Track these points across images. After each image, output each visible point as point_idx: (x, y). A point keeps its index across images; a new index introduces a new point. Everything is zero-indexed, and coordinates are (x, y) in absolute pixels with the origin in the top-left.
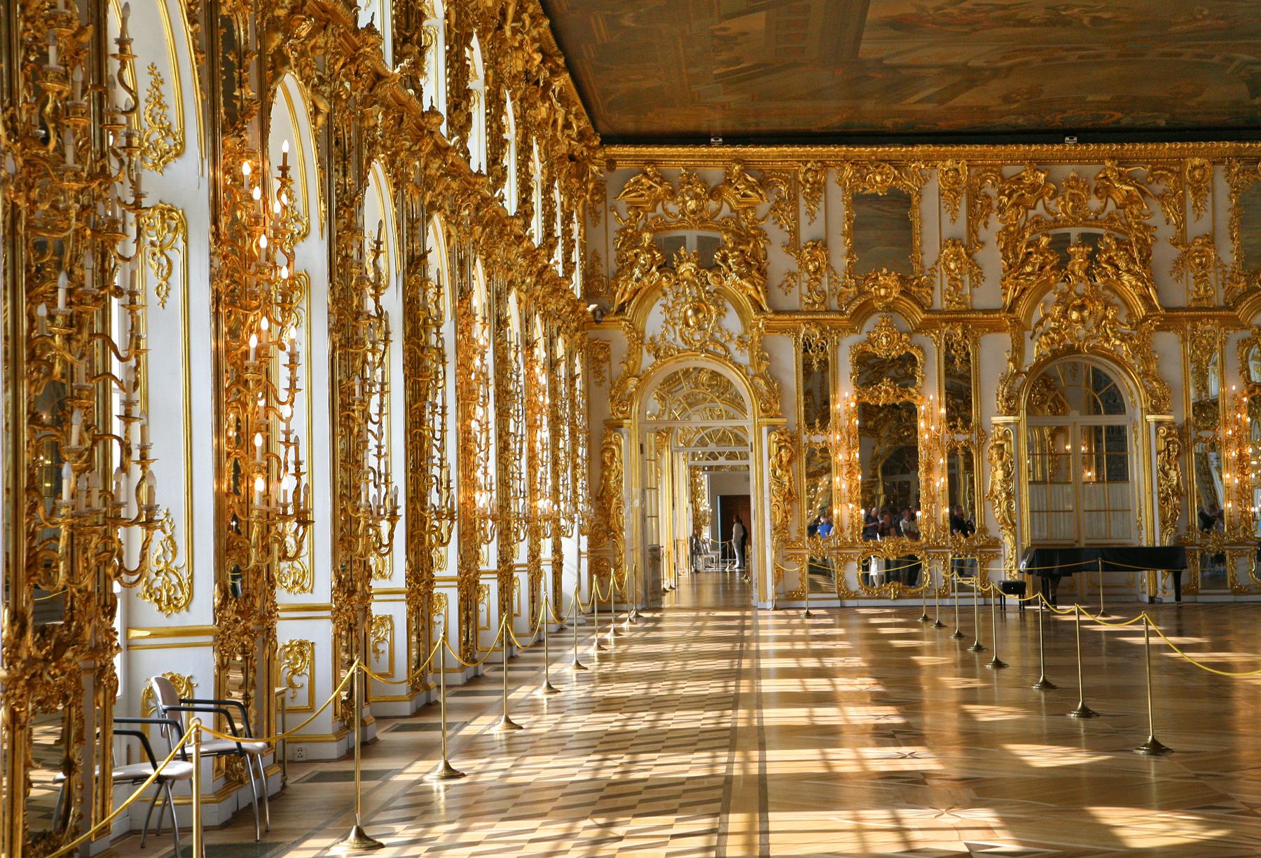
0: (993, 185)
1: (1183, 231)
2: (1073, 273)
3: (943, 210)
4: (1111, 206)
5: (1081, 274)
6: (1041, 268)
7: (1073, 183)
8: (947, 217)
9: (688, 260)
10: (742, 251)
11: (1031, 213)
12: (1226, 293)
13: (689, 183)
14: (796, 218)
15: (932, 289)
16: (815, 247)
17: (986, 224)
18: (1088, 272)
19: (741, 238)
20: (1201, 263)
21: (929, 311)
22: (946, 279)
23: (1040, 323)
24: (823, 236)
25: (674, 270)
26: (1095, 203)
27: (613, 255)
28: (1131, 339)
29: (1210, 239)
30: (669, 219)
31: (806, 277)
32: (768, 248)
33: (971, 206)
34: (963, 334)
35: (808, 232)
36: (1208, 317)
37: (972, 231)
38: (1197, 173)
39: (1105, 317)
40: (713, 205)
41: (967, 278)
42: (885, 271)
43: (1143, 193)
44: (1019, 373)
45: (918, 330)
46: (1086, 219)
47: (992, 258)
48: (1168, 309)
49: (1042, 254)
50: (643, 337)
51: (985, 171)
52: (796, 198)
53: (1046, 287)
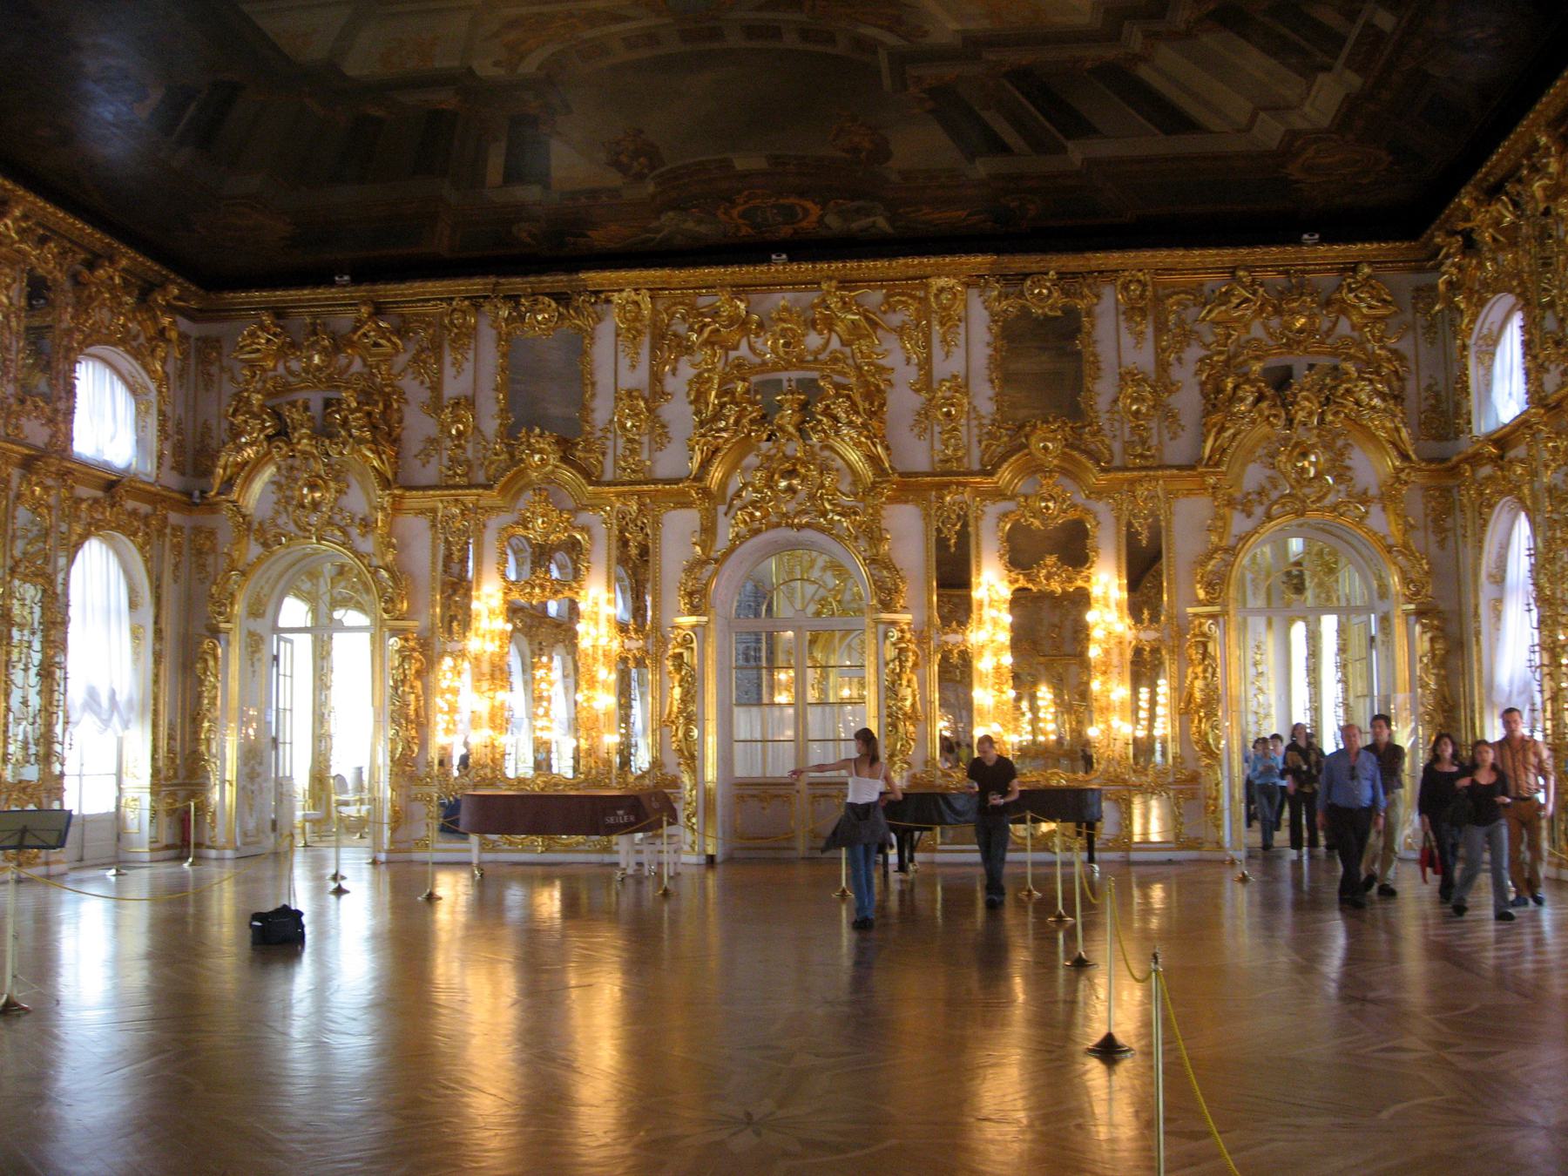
0: (684, 318)
1: (929, 374)
2: (781, 428)
3: (621, 355)
4: (835, 343)
5: (791, 429)
6: (737, 423)
7: (785, 315)
8: (624, 363)
9: (302, 426)
10: (369, 414)
11: (733, 354)
12: (983, 453)
13: (316, 334)
14: (441, 370)
15: (604, 454)
16: (458, 403)
17: (674, 371)
18: (800, 430)
19: (366, 397)
20: (948, 414)
21: (598, 483)
22: (621, 442)
23: (738, 495)
24: (470, 393)
25: (289, 443)
26: (813, 340)
27: (225, 425)
28: (856, 513)
29: (962, 385)
30: (291, 379)
31: (449, 443)
32: (406, 409)
33: (654, 348)
34: (640, 510)
35: (454, 386)
36: (959, 484)
37: (656, 377)
38: (943, 296)
39: (822, 486)
40: (342, 360)
41: (645, 439)
42: (537, 431)
43: (874, 325)
44: (706, 562)
45: (584, 508)
46: (801, 360)
47: (678, 412)
48: (901, 475)
49: (737, 404)
50: (250, 524)
51: (675, 304)
52: (440, 347)
53: (745, 446)
